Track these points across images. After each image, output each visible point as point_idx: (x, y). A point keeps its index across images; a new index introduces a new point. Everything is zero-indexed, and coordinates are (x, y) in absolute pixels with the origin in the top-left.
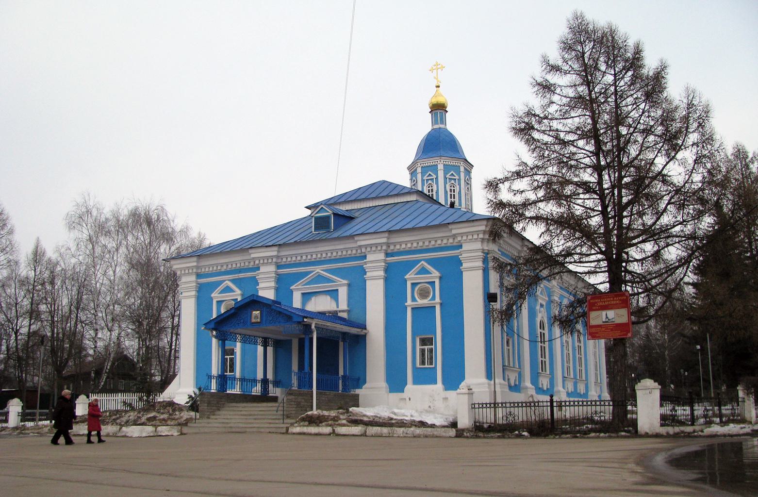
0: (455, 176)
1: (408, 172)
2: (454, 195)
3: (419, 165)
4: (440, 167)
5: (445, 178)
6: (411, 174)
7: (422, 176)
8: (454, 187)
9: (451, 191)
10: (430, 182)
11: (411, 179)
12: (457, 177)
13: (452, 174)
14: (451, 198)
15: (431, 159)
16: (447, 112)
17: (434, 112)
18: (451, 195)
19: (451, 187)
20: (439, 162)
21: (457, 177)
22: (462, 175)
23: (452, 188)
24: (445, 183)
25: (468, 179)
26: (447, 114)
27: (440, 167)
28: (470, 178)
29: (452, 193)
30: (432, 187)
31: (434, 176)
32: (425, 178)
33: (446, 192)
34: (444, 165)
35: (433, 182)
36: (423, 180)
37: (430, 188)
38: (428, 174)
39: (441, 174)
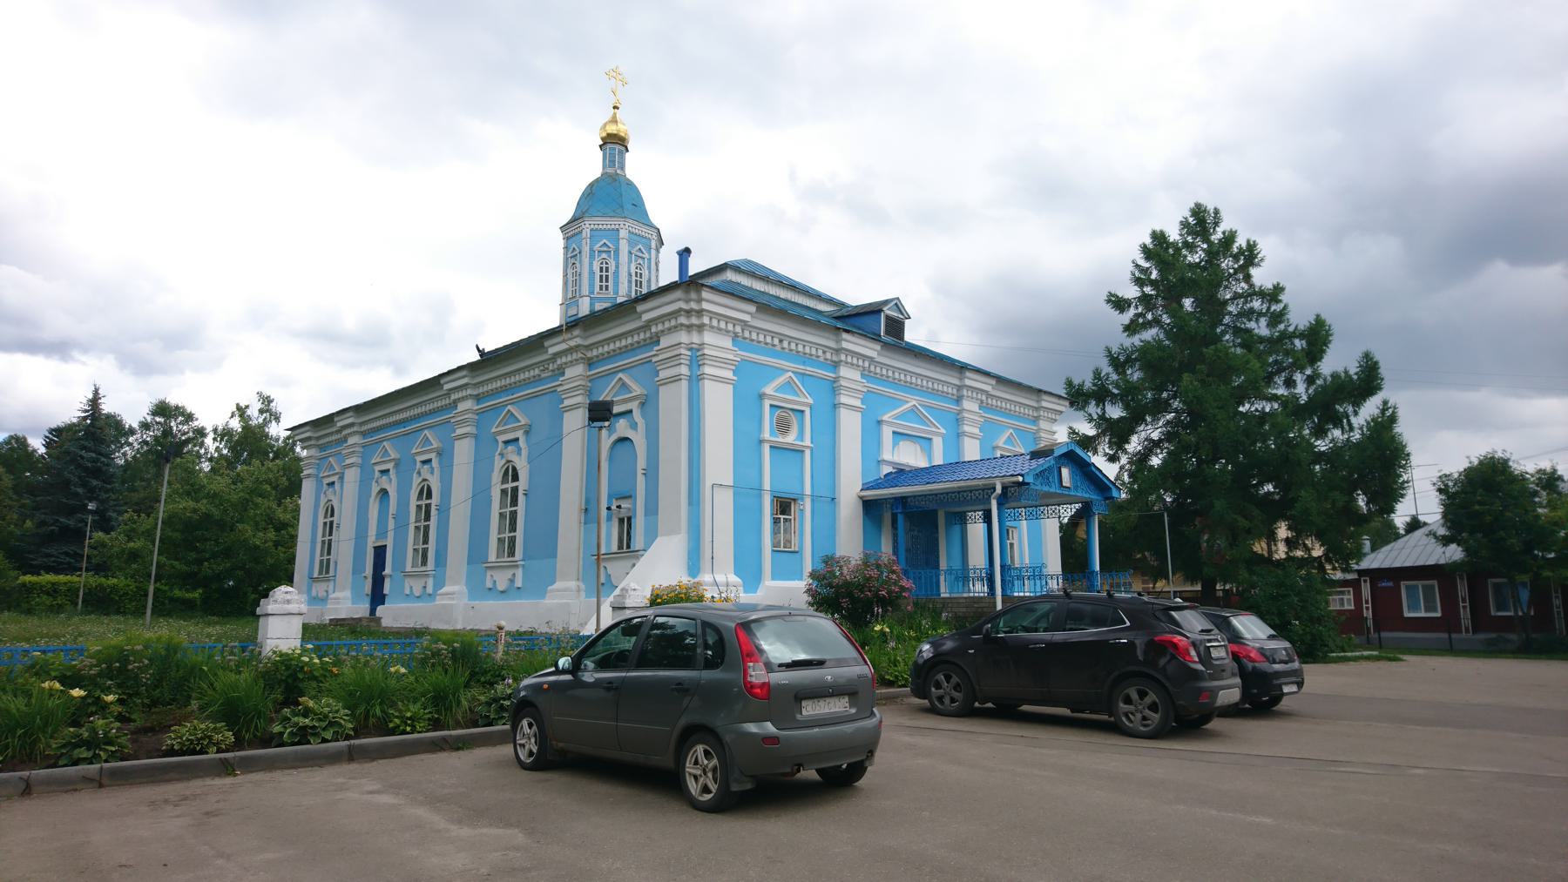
0: (643, 253)
1: (560, 236)
3: (587, 226)
4: (623, 233)
6: (567, 239)
8: (640, 269)
11: (566, 248)
13: (640, 249)
14: (636, 286)
15: (608, 219)
17: (609, 146)
19: (637, 268)
20: (622, 226)
21: (646, 256)
23: (639, 271)
24: (630, 262)
30: (606, 263)
34: (629, 232)
35: (610, 256)
36: (592, 250)
38: (602, 243)
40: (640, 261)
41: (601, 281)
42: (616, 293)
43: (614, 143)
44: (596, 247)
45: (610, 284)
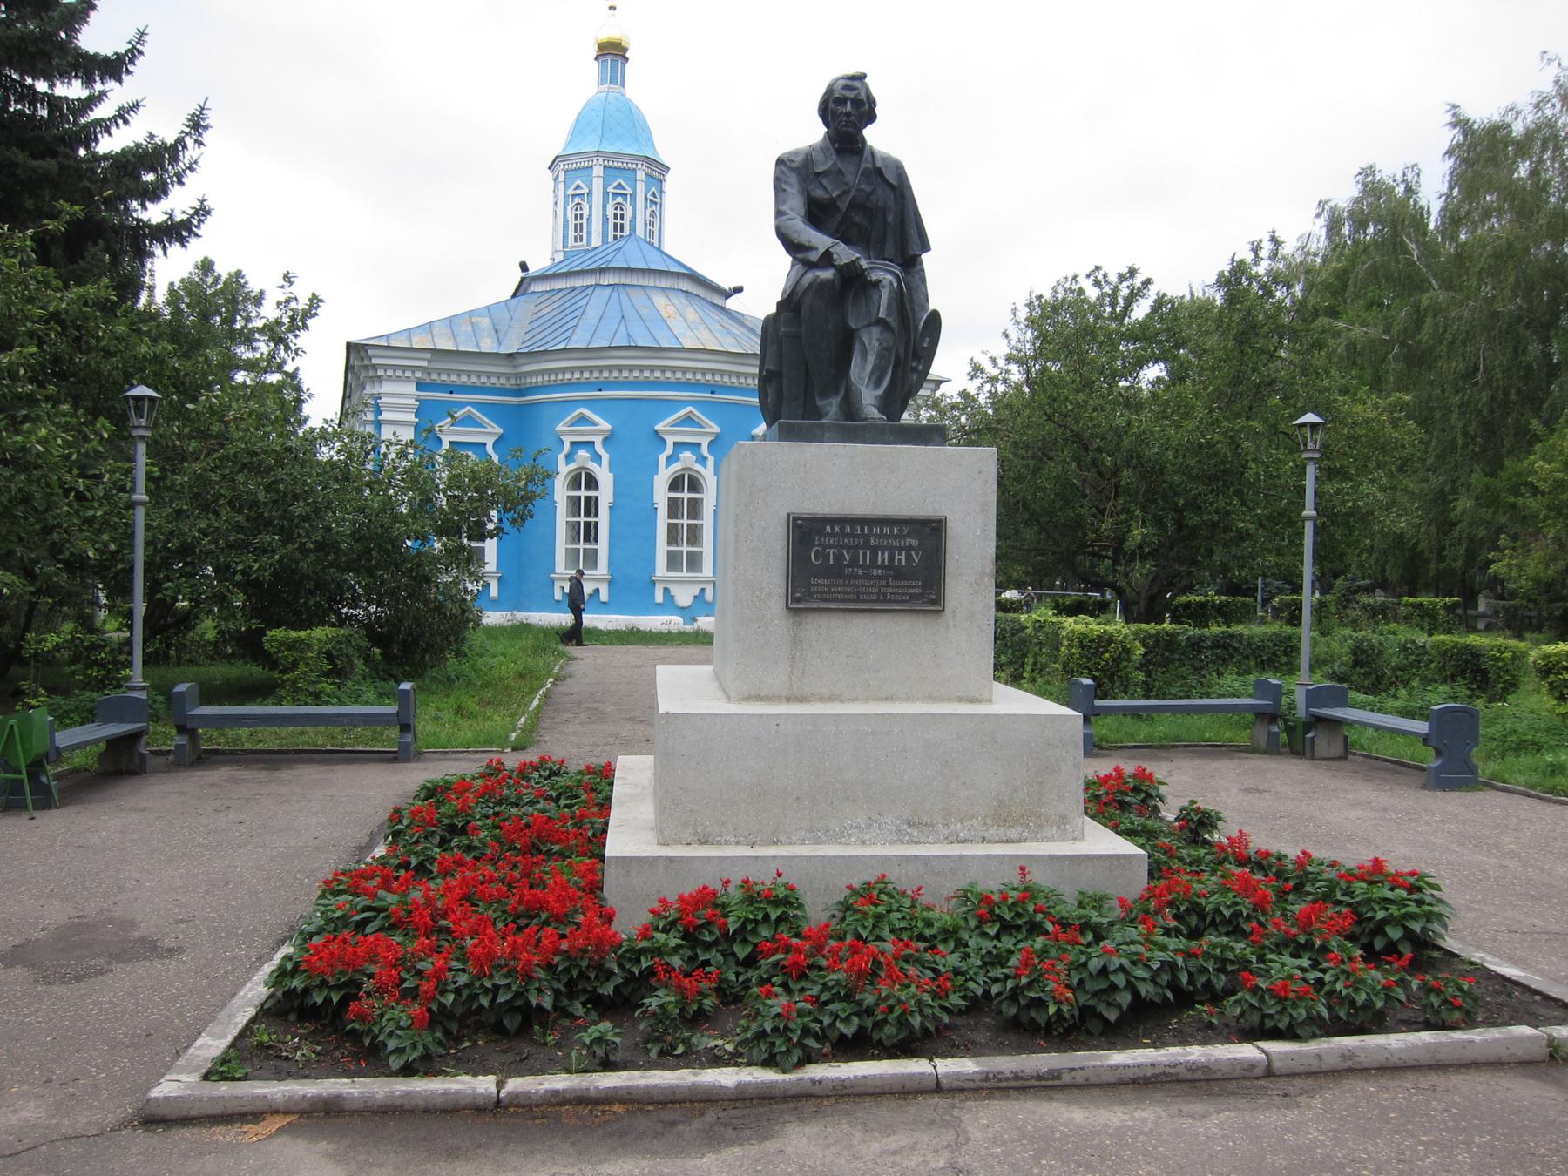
2: (622, 225)
5: (606, 193)
7: (566, 188)
9: (616, 217)
10: (577, 200)
12: (629, 191)
16: (627, 59)
18: (616, 225)
21: (629, 191)
22: (640, 187)
23: (619, 212)
25: (654, 195)
26: (628, 66)
27: (598, 171)
28: (661, 192)
29: (619, 221)
31: (586, 190)
32: (570, 192)
33: (605, 220)
37: (579, 212)
39: (598, 185)
40: (620, 199)
41: (616, 230)
42: (589, 242)
43: (612, 53)
44: (610, 189)
45: (584, 234)
